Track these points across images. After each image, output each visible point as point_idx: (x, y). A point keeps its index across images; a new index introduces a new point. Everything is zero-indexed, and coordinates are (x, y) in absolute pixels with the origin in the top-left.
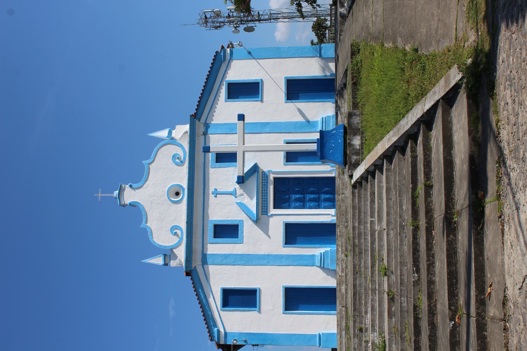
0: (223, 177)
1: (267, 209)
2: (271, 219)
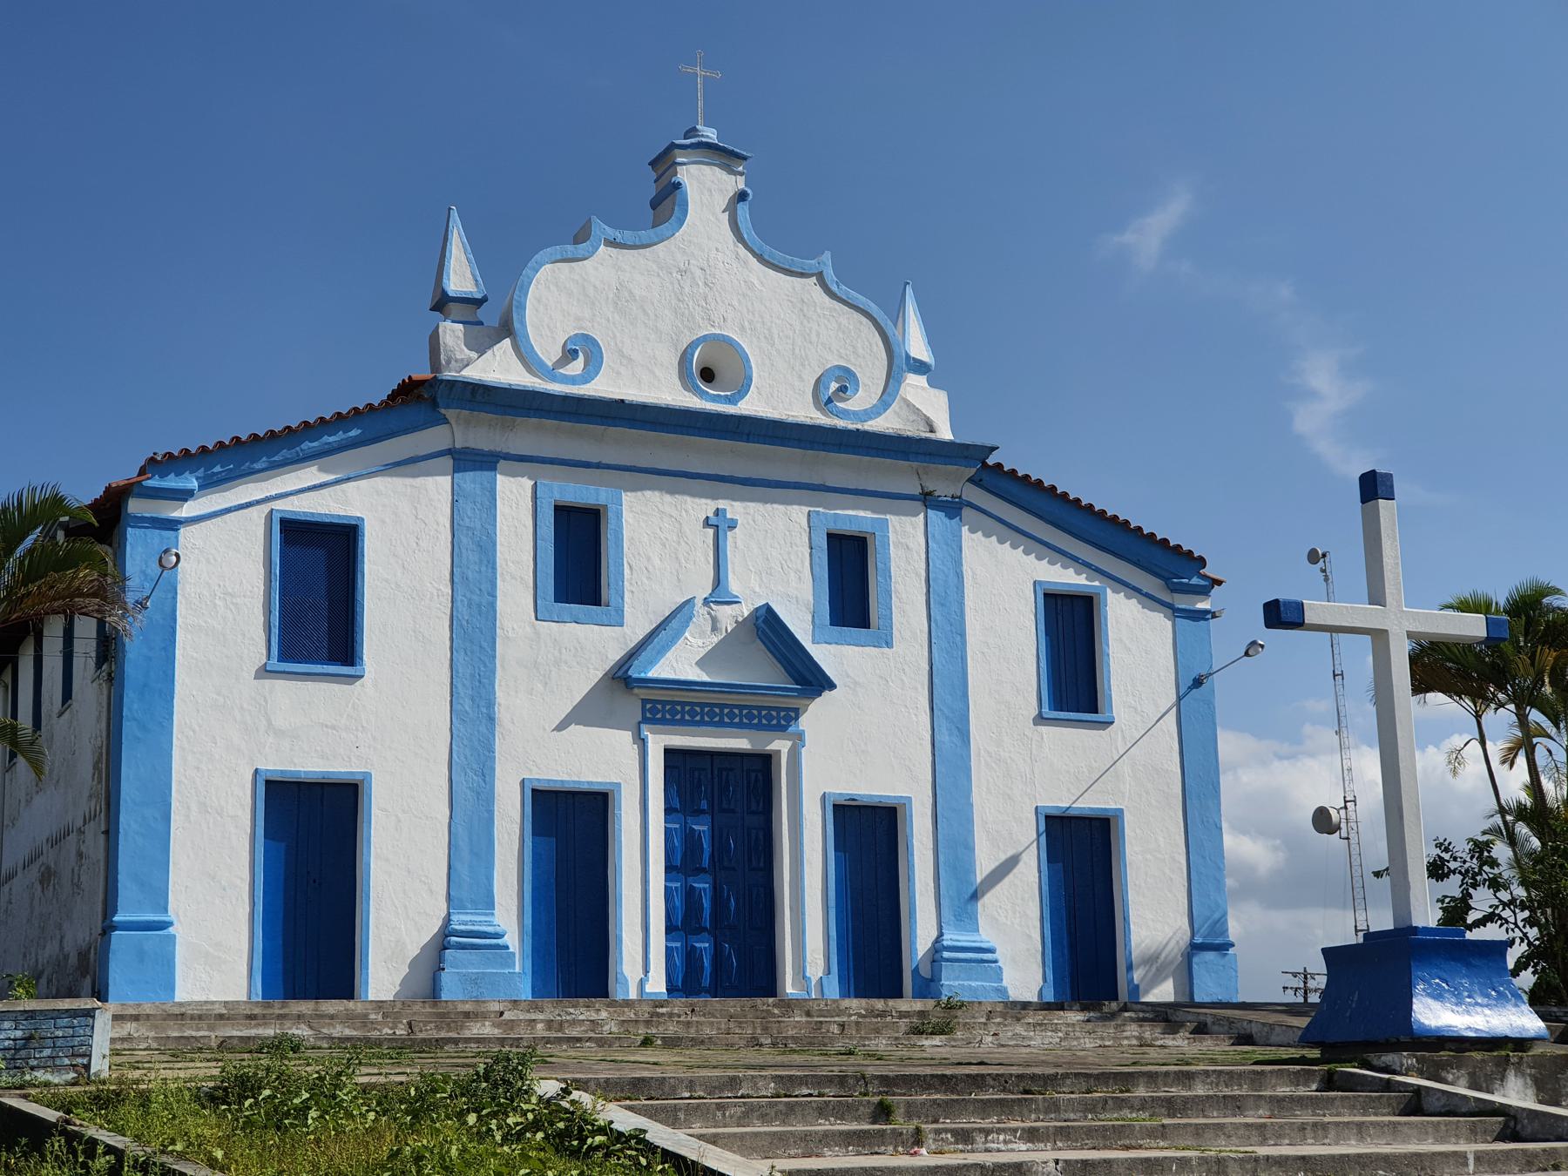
0: (776, 556)
1: (663, 721)
2: (627, 736)
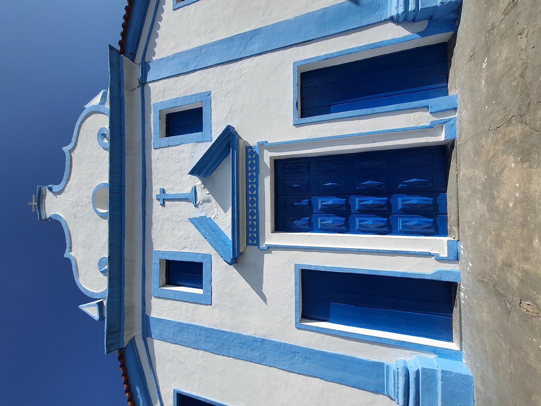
2: (267, 257)
